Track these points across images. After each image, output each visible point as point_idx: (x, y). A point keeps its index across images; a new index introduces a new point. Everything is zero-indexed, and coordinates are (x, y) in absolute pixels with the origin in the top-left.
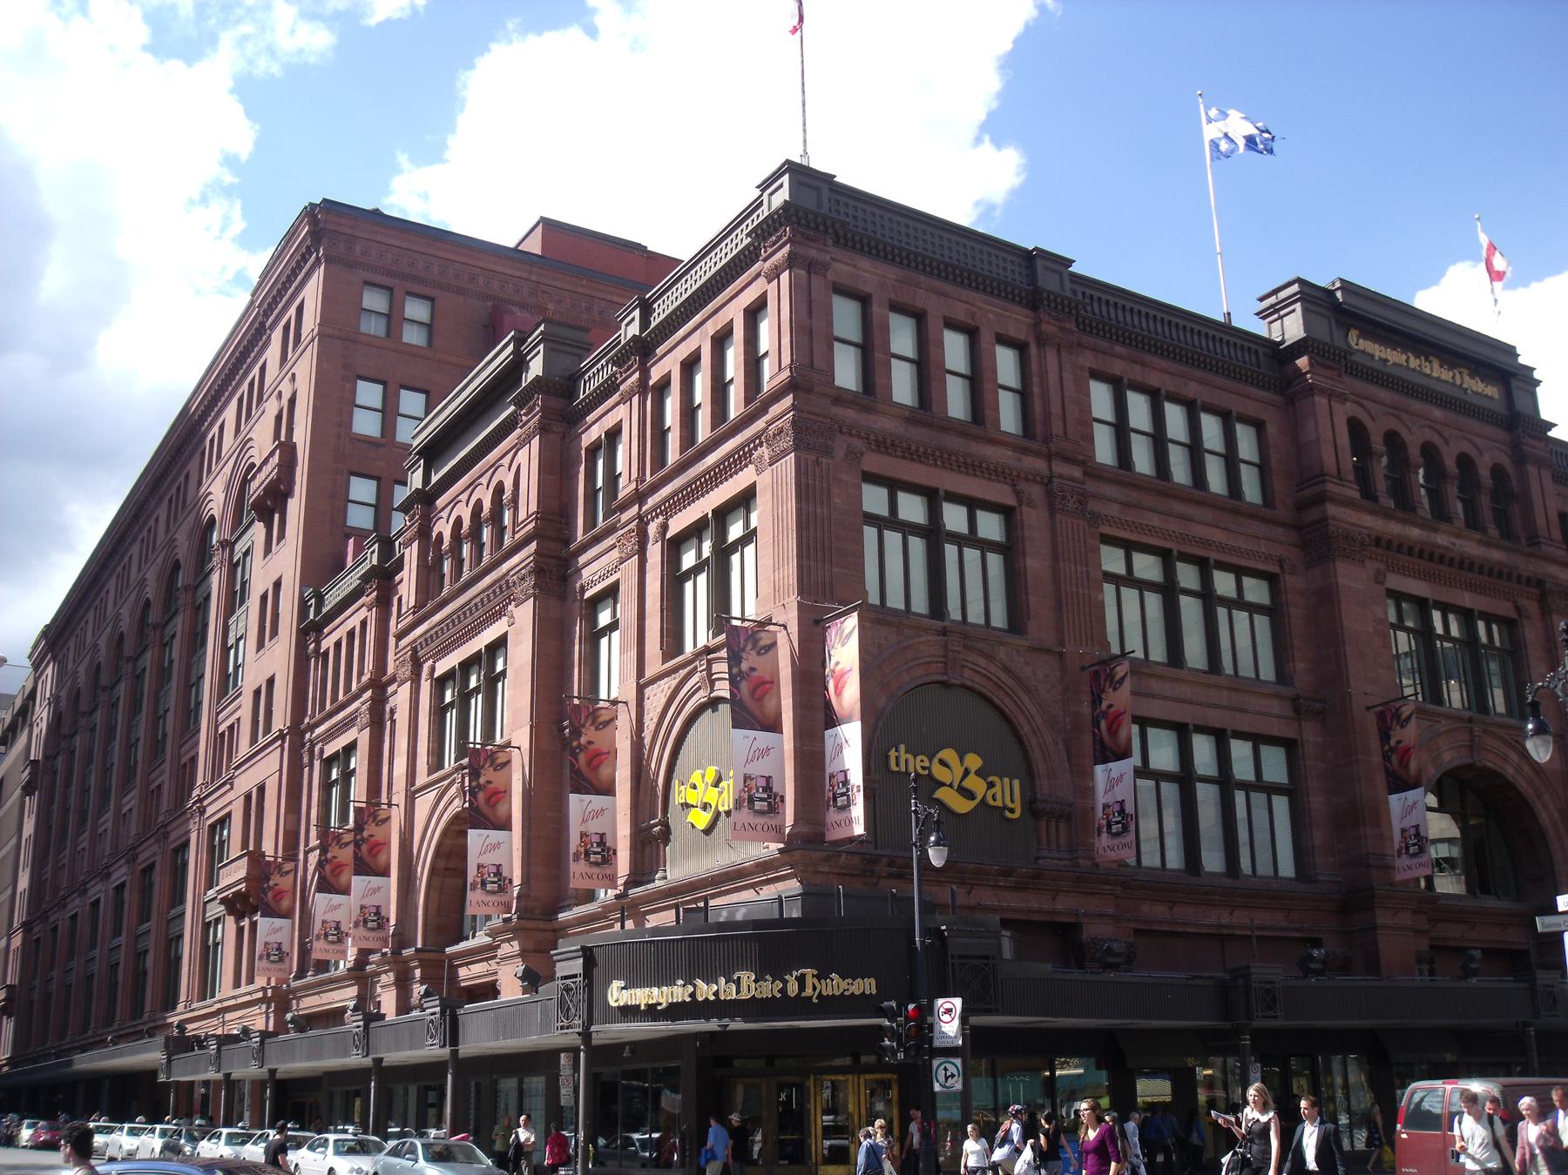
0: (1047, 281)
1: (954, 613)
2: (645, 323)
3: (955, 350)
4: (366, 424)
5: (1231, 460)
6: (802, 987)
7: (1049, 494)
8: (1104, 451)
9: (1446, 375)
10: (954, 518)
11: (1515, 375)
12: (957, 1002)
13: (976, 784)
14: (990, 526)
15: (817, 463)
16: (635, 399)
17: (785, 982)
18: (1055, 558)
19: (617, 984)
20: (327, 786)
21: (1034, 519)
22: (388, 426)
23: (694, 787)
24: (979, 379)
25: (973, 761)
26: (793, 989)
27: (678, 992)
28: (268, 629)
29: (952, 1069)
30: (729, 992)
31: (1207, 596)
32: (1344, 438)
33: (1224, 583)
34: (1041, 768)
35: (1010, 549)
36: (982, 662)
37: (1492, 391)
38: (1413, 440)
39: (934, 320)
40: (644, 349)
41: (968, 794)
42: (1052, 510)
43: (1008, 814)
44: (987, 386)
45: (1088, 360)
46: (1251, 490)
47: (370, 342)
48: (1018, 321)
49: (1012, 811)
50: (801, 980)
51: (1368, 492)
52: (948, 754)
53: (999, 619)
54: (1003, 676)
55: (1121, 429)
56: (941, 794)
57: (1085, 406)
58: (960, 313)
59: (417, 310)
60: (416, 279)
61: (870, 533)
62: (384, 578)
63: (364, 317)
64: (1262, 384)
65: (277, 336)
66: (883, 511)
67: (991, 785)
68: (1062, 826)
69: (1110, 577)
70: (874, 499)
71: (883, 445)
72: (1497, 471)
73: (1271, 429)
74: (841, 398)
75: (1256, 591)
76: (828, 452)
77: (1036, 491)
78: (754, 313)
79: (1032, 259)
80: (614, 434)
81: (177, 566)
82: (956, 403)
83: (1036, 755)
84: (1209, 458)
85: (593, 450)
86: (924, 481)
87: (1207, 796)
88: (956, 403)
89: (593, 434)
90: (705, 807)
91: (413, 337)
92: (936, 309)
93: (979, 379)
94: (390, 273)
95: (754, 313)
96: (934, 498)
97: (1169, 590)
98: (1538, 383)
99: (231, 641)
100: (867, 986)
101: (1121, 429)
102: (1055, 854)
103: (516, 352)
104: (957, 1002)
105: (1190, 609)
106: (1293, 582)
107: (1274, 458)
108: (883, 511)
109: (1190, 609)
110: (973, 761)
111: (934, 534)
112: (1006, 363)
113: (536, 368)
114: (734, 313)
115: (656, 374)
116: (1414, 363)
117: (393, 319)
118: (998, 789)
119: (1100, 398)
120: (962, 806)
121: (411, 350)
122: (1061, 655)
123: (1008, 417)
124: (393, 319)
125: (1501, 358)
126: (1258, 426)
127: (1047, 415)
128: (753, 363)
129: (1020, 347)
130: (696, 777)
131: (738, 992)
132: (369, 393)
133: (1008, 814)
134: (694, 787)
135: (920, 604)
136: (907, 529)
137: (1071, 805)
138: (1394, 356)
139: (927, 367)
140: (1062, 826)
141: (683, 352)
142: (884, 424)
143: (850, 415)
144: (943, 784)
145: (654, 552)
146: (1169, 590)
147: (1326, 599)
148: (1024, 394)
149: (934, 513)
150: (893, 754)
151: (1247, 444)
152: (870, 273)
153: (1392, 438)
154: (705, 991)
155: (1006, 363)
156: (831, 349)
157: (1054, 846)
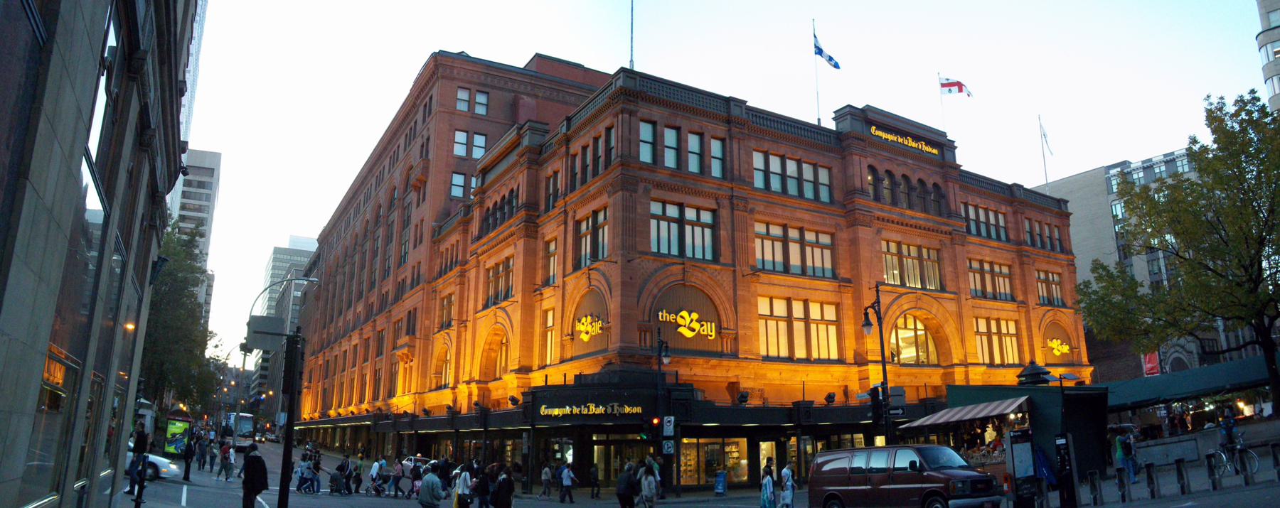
0: (735, 111)
1: (689, 253)
2: (568, 128)
3: (693, 142)
4: (459, 150)
5: (816, 183)
7: (732, 204)
8: (759, 182)
9: (914, 145)
10: (690, 214)
12: (672, 418)
13: (696, 326)
14: (706, 217)
18: (733, 230)
21: (724, 213)
22: (469, 151)
24: (703, 155)
25: (695, 316)
27: (567, 410)
28: (418, 241)
31: (802, 243)
33: (810, 237)
34: (724, 318)
35: (714, 227)
37: (935, 151)
38: (898, 172)
39: (684, 130)
40: (567, 140)
41: (693, 330)
42: (732, 210)
44: (706, 159)
45: (753, 144)
46: (824, 195)
47: (461, 113)
48: (721, 130)
51: (877, 198)
52: (684, 313)
53: (709, 256)
55: (767, 173)
57: (750, 163)
58: (696, 129)
59: (481, 98)
60: (484, 85)
61: (653, 223)
62: (466, 223)
64: (831, 151)
65: (421, 108)
66: (660, 212)
69: (759, 236)
70: (656, 208)
71: (659, 185)
72: (935, 185)
73: (835, 170)
74: (644, 166)
75: (825, 239)
76: (636, 191)
77: (726, 202)
78: (608, 129)
79: (729, 100)
80: (556, 173)
81: (380, 207)
82: (693, 165)
83: (722, 313)
84: (805, 184)
85: (548, 179)
86: (677, 200)
87: (799, 327)
88: (693, 165)
89: (550, 171)
91: (481, 110)
92: (684, 124)
93: (703, 155)
94: (470, 82)
95: (608, 129)
96: (681, 207)
97: (785, 241)
101: (767, 173)
103: (518, 134)
104: (672, 418)
107: (835, 183)
108: (660, 212)
111: (681, 221)
112: (716, 148)
114: (601, 128)
115: (572, 151)
116: (900, 140)
117: (471, 103)
119: (758, 161)
120: (689, 334)
121: (479, 117)
123: (716, 170)
124: (471, 103)
125: (940, 139)
126: (830, 169)
127: (732, 169)
129: (723, 140)
130: (584, 320)
132: (461, 137)
135: (675, 251)
136: (670, 220)
138: (891, 137)
139: (680, 150)
142: (660, 177)
143: (646, 174)
146: (785, 241)
147: (854, 242)
148: (723, 160)
149: (682, 212)
151: (824, 176)
152: (657, 113)
153: (889, 173)
154: (576, 410)
155: (716, 148)
156: (638, 146)
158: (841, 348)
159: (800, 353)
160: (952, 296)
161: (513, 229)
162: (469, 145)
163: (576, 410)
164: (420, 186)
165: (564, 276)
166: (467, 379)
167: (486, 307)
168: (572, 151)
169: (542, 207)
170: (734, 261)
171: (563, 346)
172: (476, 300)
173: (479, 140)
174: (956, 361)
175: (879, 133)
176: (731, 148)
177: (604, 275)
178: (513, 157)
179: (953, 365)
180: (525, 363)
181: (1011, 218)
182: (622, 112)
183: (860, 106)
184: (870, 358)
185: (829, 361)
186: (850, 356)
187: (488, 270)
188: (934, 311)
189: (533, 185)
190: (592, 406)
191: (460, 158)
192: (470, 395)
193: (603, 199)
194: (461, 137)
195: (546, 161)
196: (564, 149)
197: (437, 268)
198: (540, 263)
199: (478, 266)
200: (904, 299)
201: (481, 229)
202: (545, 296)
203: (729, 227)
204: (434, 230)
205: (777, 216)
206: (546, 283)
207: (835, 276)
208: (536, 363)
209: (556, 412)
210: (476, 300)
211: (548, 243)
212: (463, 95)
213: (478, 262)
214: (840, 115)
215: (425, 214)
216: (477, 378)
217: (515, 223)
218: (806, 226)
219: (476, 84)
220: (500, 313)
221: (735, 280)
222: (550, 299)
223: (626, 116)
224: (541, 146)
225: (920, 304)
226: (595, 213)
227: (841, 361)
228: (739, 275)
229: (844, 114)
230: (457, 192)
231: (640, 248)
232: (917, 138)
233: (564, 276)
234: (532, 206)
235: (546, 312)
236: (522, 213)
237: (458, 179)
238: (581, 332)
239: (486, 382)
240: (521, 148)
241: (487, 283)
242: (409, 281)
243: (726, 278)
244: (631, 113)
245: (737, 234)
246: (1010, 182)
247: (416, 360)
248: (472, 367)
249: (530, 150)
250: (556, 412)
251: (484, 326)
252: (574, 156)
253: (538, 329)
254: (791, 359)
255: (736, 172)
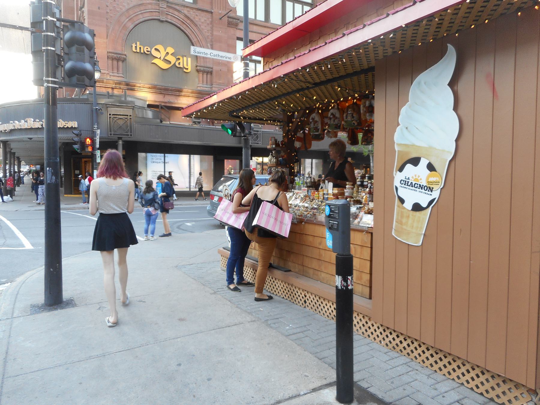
25: (170, 50)
36: (176, 13)
43: (185, 70)
49: (187, 69)
54: (186, 19)
56: (155, 61)
67: (179, 59)
68: (209, 76)
102: (206, 86)
110: (170, 50)
118: (181, 61)
122: (212, 13)
133: (185, 70)
137: (212, 68)
140: (209, 76)
144: (157, 58)
150: (134, 45)
157: (205, 83)
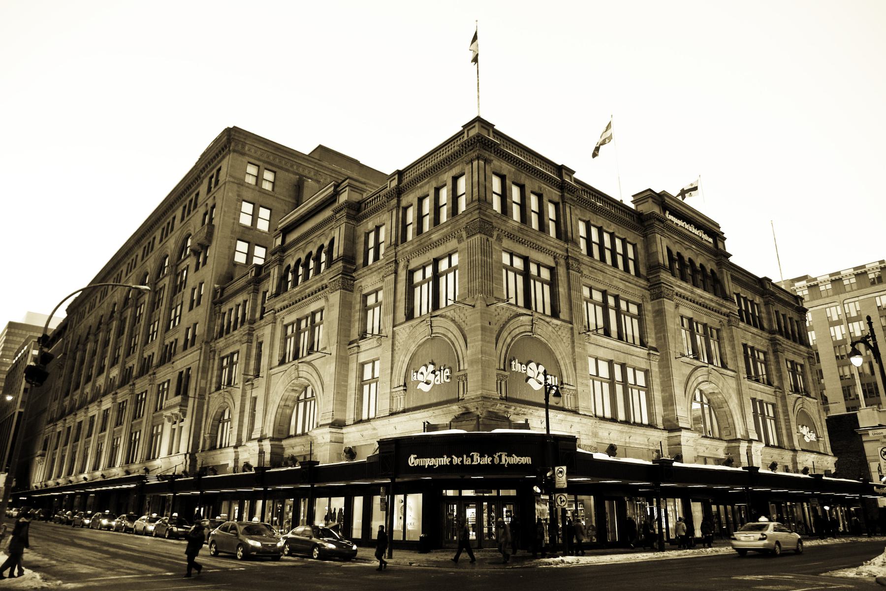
6: (501, 460)
11: (718, 235)
15: (488, 240)
16: (394, 212)
17: (493, 458)
19: (412, 457)
20: (221, 368)
21: (561, 271)
23: (422, 373)
26: (497, 461)
27: (445, 461)
29: (563, 498)
30: (467, 461)
32: (666, 253)
37: (711, 240)
42: (568, 268)
48: (555, 194)
50: (500, 457)
53: (548, 311)
59: (268, 176)
63: (247, 176)
71: (510, 236)
73: (639, 246)
76: (492, 236)
79: (561, 170)
83: (563, 368)
89: (371, 225)
90: (427, 383)
91: (267, 186)
98: (725, 239)
99: (174, 306)
100: (526, 460)
105: (612, 314)
106: (648, 307)
107: (640, 258)
109: (612, 314)
113: (343, 198)
116: (687, 226)
117: (259, 178)
121: (264, 192)
124: (259, 178)
126: (634, 246)
127: (566, 232)
128: (455, 198)
129: (556, 205)
131: (472, 461)
134: (422, 373)
138: (680, 223)
141: (419, 193)
145: (402, 275)
147: (660, 313)
152: (506, 168)
154: (456, 460)
158: (650, 414)
159: (621, 416)
160: (732, 373)
161: (325, 282)
162: (255, 216)
163: (456, 460)
164: (201, 249)
165: (394, 326)
166: (259, 436)
167: (282, 362)
168: (404, 203)
169: (361, 261)
170: (572, 318)
171: (392, 399)
172: (271, 356)
173: (264, 213)
174: (739, 436)
175: (671, 217)
176: (564, 210)
177: (453, 321)
178: (328, 213)
179: (737, 440)
180: (338, 417)
181: (763, 309)
182: (478, 158)
183: (658, 192)
184: (681, 425)
185: (641, 425)
186: (659, 421)
187: (286, 326)
188: (721, 385)
189: (351, 240)
190: (476, 456)
191: (246, 227)
192: (261, 453)
193: (453, 244)
194: (247, 208)
195: (365, 216)
196: (394, 202)
197: (217, 328)
198: (357, 316)
199: (274, 322)
200: (698, 373)
201: (279, 287)
202: (363, 348)
203: (566, 286)
204: (215, 291)
205: (599, 282)
206: (363, 335)
207: (643, 344)
208: (350, 417)
209: (428, 462)
210: (271, 356)
211: (365, 297)
212: (252, 170)
213: (275, 319)
214: (639, 198)
215: (203, 278)
216: (270, 435)
217: (328, 275)
218: (621, 295)
219: (264, 162)
220: (303, 367)
221: (572, 334)
222: (368, 350)
223: (482, 162)
224: (359, 203)
225: (711, 378)
226: (436, 262)
227: (652, 426)
228: (576, 332)
229: (647, 196)
230: (240, 258)
231: (496, 295)
232: (698, 227)
233: (394, 326)
234: (349, 259)
235: (362, 365)
236: (340, 264)
237: (242, 246)
238: (418, 382)
239: (280, 440)
240: (336, 205)
241: (285, 338)
242: (181, 342)
243: (565, 334)
244: (487, 161)
245: (573, 293)
246: (760, 276)
247: (187, 420)
248: (265, 425)
249: (349, 205)
250: (428, 462)
251: (279, 384)
252: (405, 209)
253: (353, 382)
254: (614, 420)
255: (569, 235)
